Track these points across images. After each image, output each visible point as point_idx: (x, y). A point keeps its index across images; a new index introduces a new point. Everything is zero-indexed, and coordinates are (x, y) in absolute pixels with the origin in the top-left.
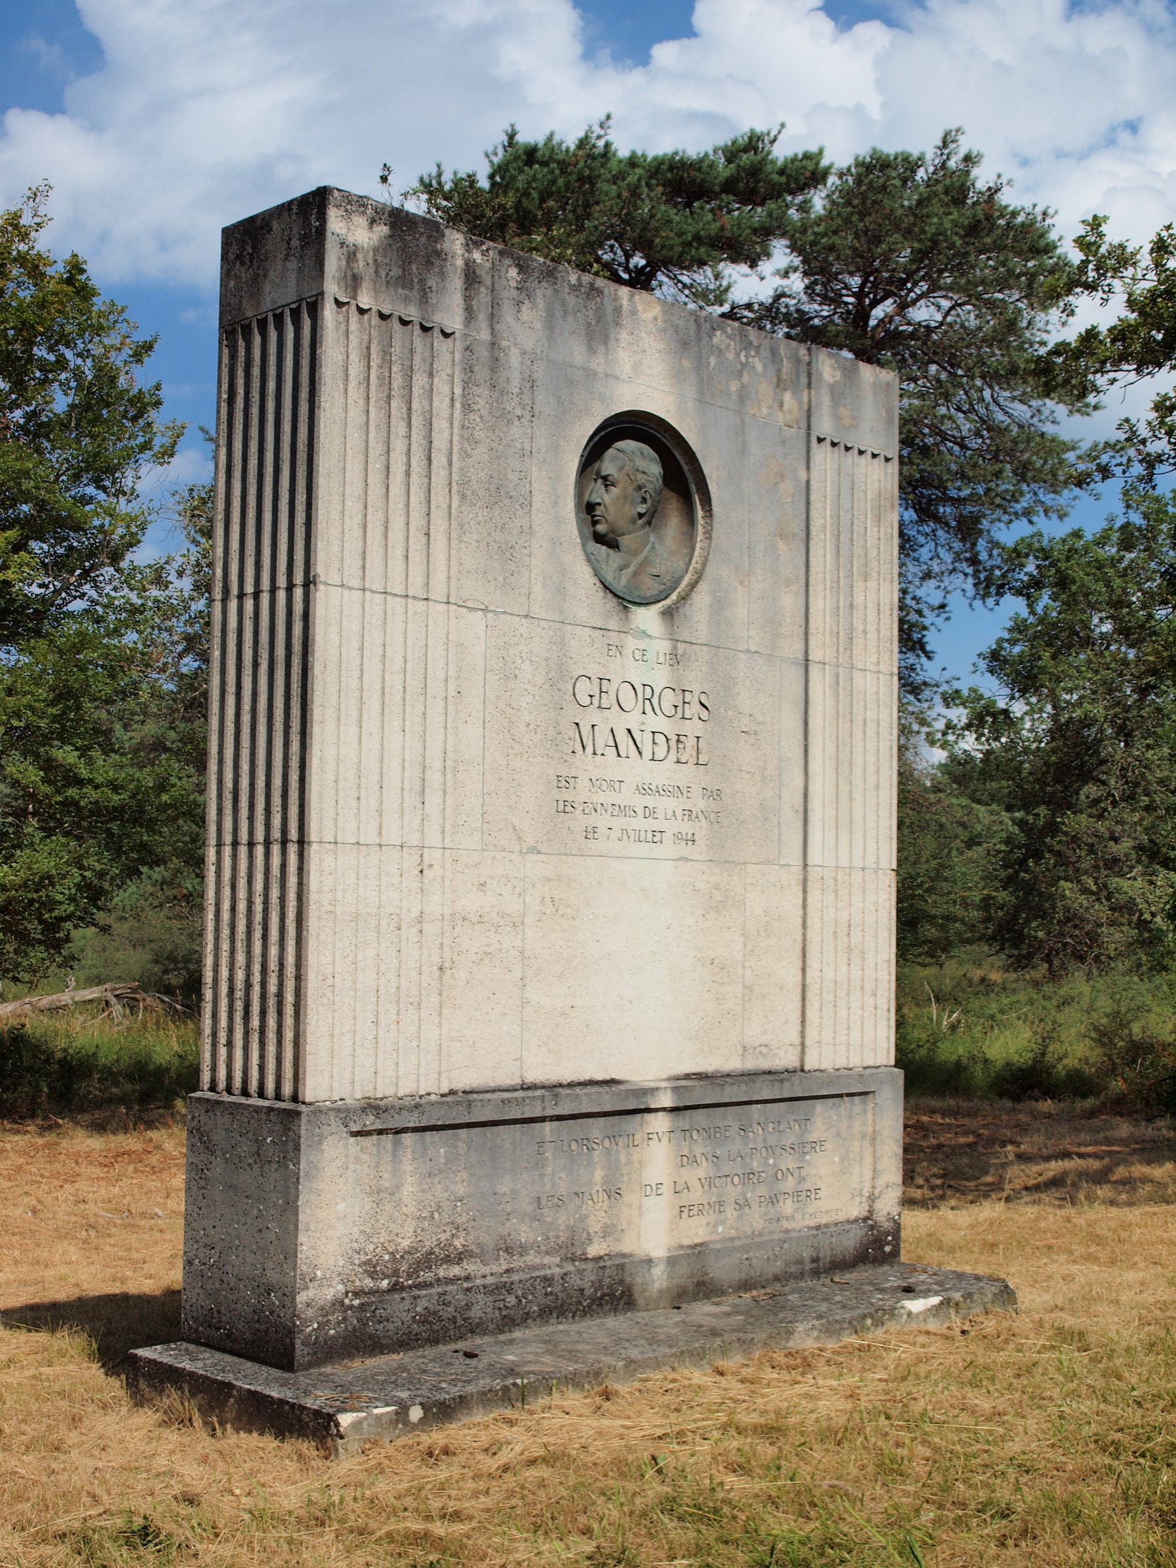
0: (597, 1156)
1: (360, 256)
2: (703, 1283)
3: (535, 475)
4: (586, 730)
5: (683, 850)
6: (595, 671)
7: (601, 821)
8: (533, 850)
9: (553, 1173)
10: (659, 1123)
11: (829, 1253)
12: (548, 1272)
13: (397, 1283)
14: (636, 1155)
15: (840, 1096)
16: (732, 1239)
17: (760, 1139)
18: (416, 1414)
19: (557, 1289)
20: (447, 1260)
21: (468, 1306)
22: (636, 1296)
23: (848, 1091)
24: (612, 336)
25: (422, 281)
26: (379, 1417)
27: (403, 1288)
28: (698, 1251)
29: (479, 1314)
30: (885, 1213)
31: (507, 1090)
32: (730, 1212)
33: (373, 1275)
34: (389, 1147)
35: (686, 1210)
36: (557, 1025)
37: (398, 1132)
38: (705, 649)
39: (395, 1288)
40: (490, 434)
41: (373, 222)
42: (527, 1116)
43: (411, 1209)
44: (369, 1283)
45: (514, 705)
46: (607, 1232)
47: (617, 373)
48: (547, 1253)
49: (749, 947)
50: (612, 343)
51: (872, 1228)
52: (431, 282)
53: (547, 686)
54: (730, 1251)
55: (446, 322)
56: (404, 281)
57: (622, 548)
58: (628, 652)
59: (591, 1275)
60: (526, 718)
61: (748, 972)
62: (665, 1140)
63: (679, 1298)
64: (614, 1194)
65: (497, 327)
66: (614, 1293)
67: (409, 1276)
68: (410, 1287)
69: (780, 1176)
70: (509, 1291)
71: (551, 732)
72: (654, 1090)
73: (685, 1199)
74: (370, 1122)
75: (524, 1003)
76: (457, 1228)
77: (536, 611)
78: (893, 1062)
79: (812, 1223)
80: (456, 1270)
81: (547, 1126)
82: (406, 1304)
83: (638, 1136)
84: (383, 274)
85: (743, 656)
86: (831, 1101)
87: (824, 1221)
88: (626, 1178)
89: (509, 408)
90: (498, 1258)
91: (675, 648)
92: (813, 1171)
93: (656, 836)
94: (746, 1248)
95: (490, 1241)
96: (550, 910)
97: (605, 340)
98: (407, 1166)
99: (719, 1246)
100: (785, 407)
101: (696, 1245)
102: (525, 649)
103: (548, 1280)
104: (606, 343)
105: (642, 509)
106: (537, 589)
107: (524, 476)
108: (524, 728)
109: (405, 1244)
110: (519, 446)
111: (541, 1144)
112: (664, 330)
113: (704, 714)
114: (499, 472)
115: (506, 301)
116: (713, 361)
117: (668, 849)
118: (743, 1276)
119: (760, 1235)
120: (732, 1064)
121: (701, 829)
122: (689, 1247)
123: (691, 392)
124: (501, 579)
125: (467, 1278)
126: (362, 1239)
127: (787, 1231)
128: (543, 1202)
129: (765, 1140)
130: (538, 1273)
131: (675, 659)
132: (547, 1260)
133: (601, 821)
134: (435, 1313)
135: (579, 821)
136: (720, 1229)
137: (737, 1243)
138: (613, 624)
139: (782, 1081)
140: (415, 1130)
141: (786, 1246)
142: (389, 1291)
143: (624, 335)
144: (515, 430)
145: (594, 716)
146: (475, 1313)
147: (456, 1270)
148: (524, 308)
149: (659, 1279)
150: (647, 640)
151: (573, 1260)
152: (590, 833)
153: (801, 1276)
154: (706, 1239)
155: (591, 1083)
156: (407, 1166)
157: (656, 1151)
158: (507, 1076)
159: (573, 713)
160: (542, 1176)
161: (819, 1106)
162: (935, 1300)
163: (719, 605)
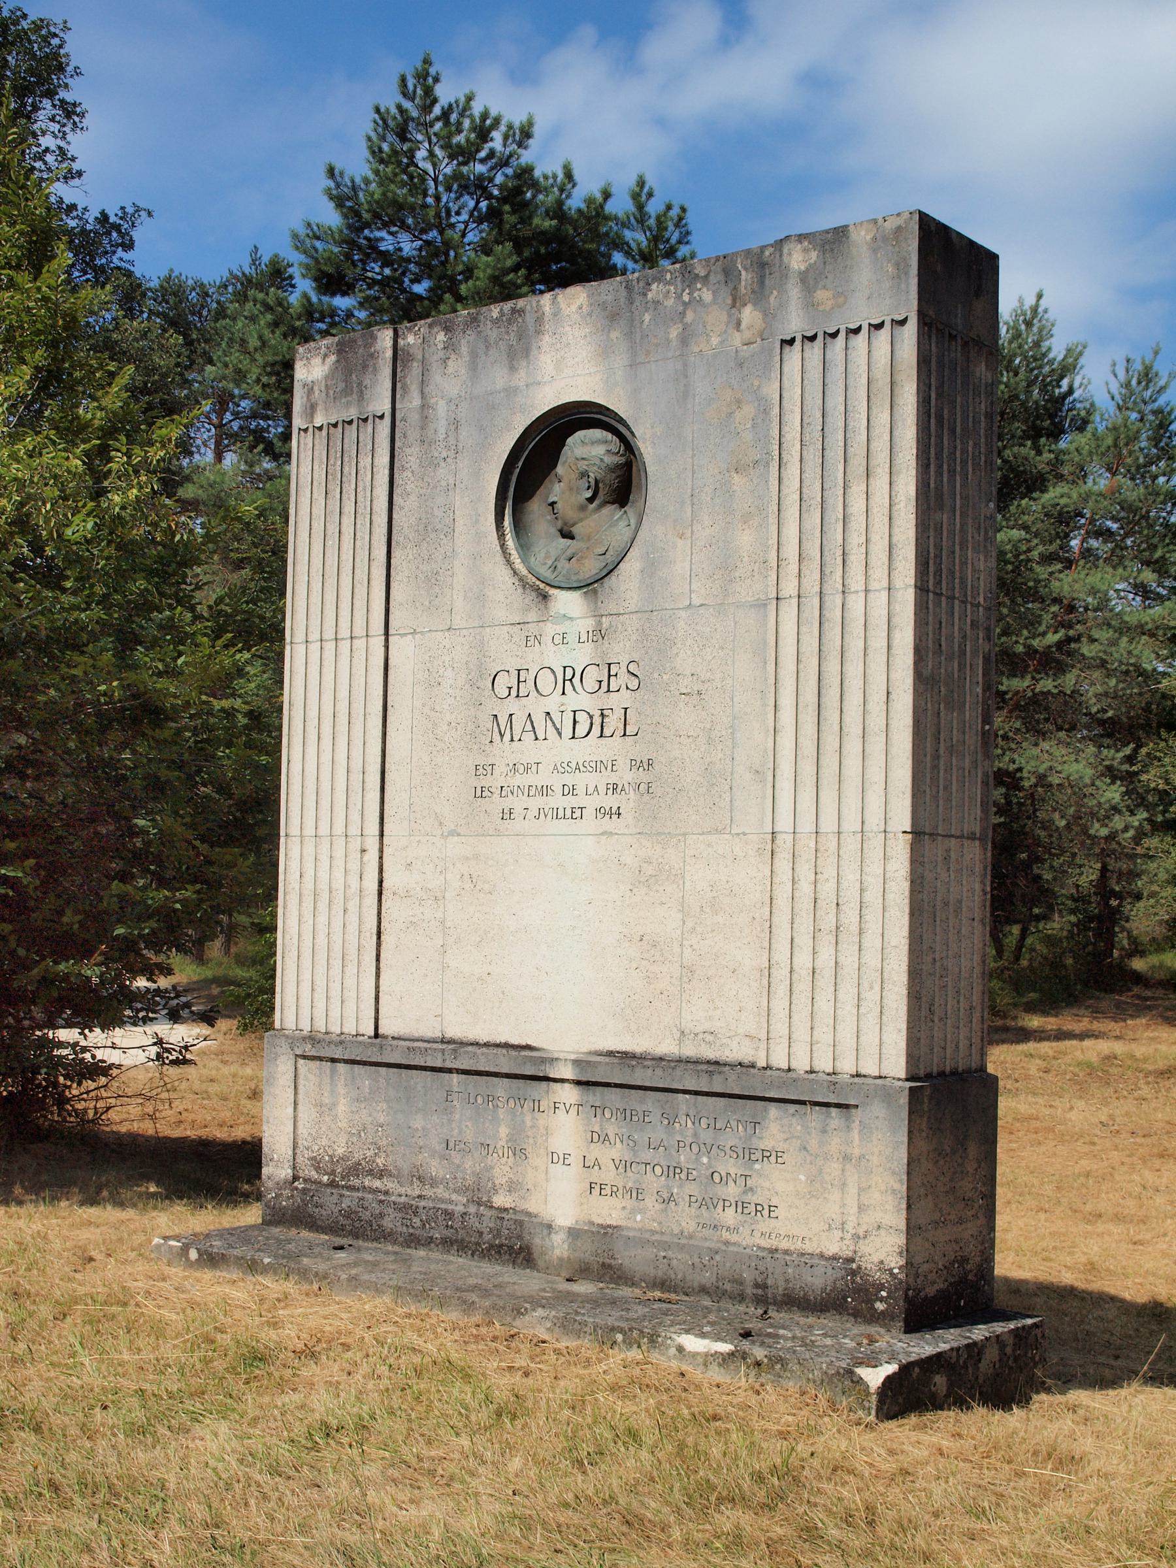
0: (501, 1113)
1: (316, 388)
2: (610, 1266)
3: (457, 504)
4: (503, 720)
5: (607, 824)
6: (512, 664)
7: (517, 803)
8: (453, 833)
9: (461, 1121)
10: (568, 1094)
11: (782, 1284)
12: (450, 1207)
13: (334, 1181)
14: (542, 1120)
15: (803, 1103)
16: (653, 1232)
17: (690, 1133)
18: (193, 1255)
19: (457, 1225)
20: (370, 1172)
21: (381, 1215)
22: (535, 1256)
23: (826, 1099)
24: (534, 347)
25: (360, 384)
26: (171, 1247)
27: (337, 1186)
28: (607, 1232)
29: (390, 1225)
30: (876, 1259)
31: (429, 1042)
32: (650, 1202)
33: (317, 1169)
34: (328, 1071)
35: (597, 1188)
36: (475, 990)
37: (333, 1060)
38: (634, 616)
39: (332, 1184)
40: (420, 483)
41: (325, 356)
42: (429, 1064)
43: (343, 1124)
44: (314, 1175)
45: (438, 708)
46: (512, 1187)
47: (539, 378)
48: (455, 1191)
49: (690, 924)
50: (534, 352)
51: (853, 1273)
52: (367, 382)
53: (467, 686)
54: (644, 1243)
55: (378, 408)
56: (347, 391)
57: (577, 537)
58: (547, 639)
59: (488, 1223)
60: (448, 717)
61: (687, 952)
62: (573, 1111)
63: (582, 1271)
64: (518, 1152)
65: (426, 390)
66: (512, 1245)
67: (343, 1178)
68: (343, 1187)
69: (716, 1177)
70: (415, 1213)
71: (471, 727)
72: (553, 1060)
73: (595, 1175)
74: (308, 1049)
75: (445, 967)
76: (379, 1149)
77: (458, 622)
78: (903, 1075)
79: (764, 1243)
80: (377, 1184)
81: (455, 1077)
82: (335, 1198)
83: (544, 1105)
84: (331, 392)
85: (683, 614)
86: (792, 1108)
87: (784, 1245)
88: (531, 1141)
89: (436, 454)
90: (412, 1183)
91: (600, 623)
92: (766, 1184)
93: (576, 813)
94: (667, 1246)
95: (406, 1168)
96: (468, 885)
97: (527, 352)
98: (341, 1090)
99: (631, 1234)
100: (743, 325)
101: (609, 1226)
102: (447, 658)
103: (449, 1215)
104: (527, 356)
105: (589, 494)
106: (459, 604)
107: (450, 509)
108: (445, 727)
109: (340, 1151)
110: (444, 483)
111: (449, 1093)
112: (590, 315)
113: (634, 684)
114: (427, 512)
115: (435, 365)
116: (647, 317)
117: (590, 823)
118: (660, 1274)
119: (691, 1237)
120: (667, 1047)
121: (628, 802)
122: (601, 1226)
123: (620, 361)
124: (427, 603)
125: (386, 1193)
126: (310, 1139)
127: (727, 1243)
128: (451, 1145)
129: (695, 1135)
130: (443, 1206)
131: (599, 634)
132: (454, 1197)
133: (517, 803)
134: (356, 1212)
135: (497, 804)
136: (639, 1218)
137: (656, 1237)
138: (532, 616)
139: (711, 1073)
140: (346, 1062)
141: (718, 1258)
142: (327, 1185)
143: (546, 339)
144: (442, 472)
145: (512, 705)
146: (387, 1223)
147: (377, 1184)
148: (450, 363)
149: (558, 1247)
150: (567, 623)
151: (479, 1204)
152: (507, 814)
153: (741, 1298)
154: (620, 1223)
155: (507, 1046)
156: (341, 1090)
157: (564, 1122)
158: (430, 1029)
159: (492, 706)
160: (450, 1121)
161: (773, 1110)
162: (725, 1347)
163: (651, 568)
